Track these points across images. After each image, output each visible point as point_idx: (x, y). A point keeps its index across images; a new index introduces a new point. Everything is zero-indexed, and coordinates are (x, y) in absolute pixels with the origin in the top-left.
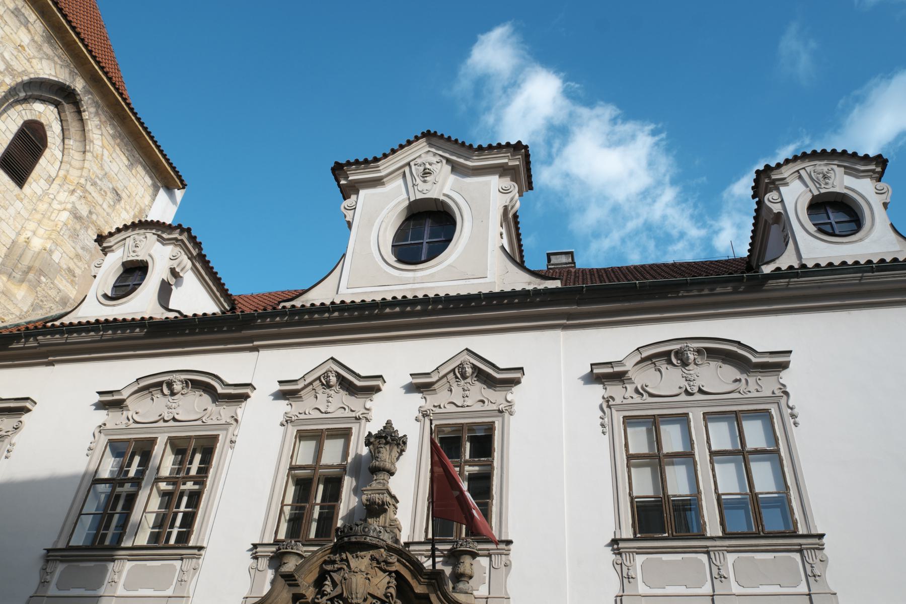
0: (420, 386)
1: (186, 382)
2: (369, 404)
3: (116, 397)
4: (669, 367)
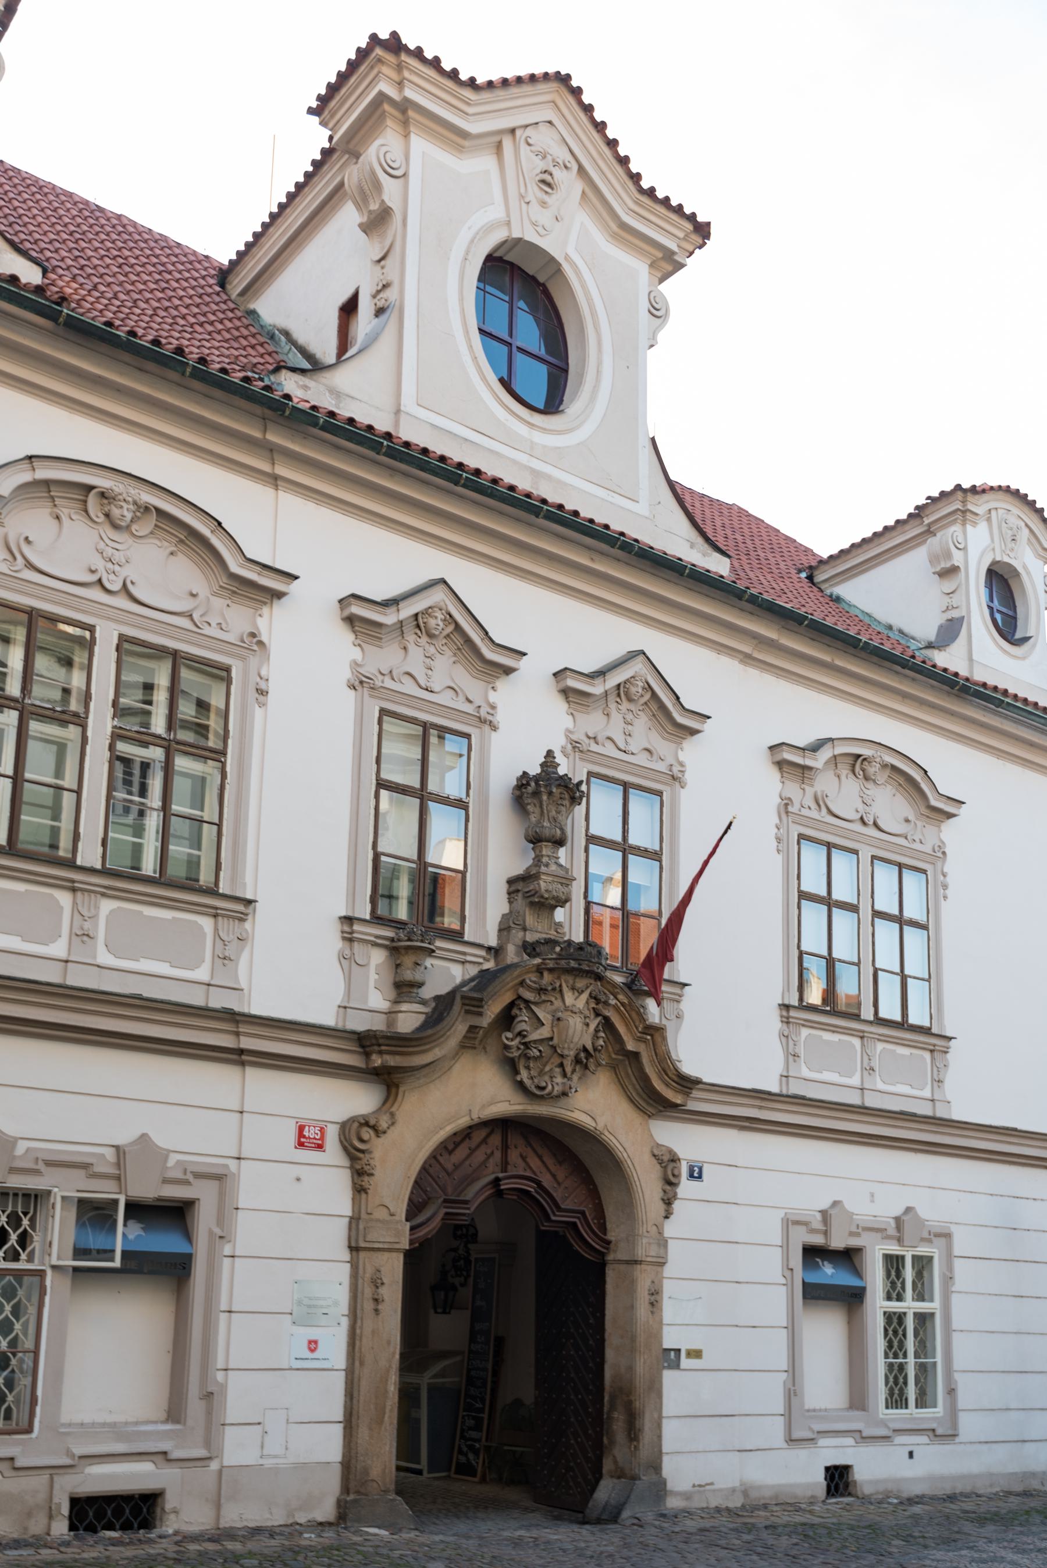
0: (571, 689)
2: (493, 697)
4: (851, 775)
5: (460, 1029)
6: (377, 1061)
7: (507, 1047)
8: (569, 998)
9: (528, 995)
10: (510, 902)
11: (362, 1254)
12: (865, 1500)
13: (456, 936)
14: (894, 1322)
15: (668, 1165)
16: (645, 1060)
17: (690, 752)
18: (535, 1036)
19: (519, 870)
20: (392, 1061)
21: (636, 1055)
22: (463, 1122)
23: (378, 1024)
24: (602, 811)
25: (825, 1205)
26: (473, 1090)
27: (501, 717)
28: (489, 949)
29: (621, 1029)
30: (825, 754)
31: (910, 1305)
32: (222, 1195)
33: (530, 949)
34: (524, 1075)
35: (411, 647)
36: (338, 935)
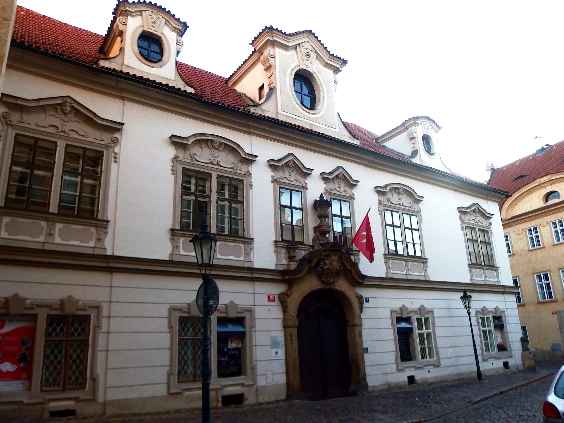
0: (325, 177)
1: (221, 144)
2: (306, 181)
3: (184, 142)
5: (307, 268)
6: (287, 277)
7: (319, 271)
8: (333, 257)
9: (323, 257)
10: (315, 233)
11: (287, 329)
12: (419, 384)
13: (302, 243)
14: (421, 336)
15: (360, 299)
16: (353, 272)
17: (355, 191)
18: (326, 268)
19: (316, 225)
20: (291, 277)
21: (350, 271)
22: (309, 291)
23: (285, 268)
24: (335, 208)
25: (400, 306)
26: (311, 284)
27: (308, 186)
28: (311, 246)
29: (346, 263)
30: (388, 188)
31: (424, 331)
32: (251, 315)
33: (322, 245)
34: (323, 278)
35: (285, 171)
36: (273, 246)
